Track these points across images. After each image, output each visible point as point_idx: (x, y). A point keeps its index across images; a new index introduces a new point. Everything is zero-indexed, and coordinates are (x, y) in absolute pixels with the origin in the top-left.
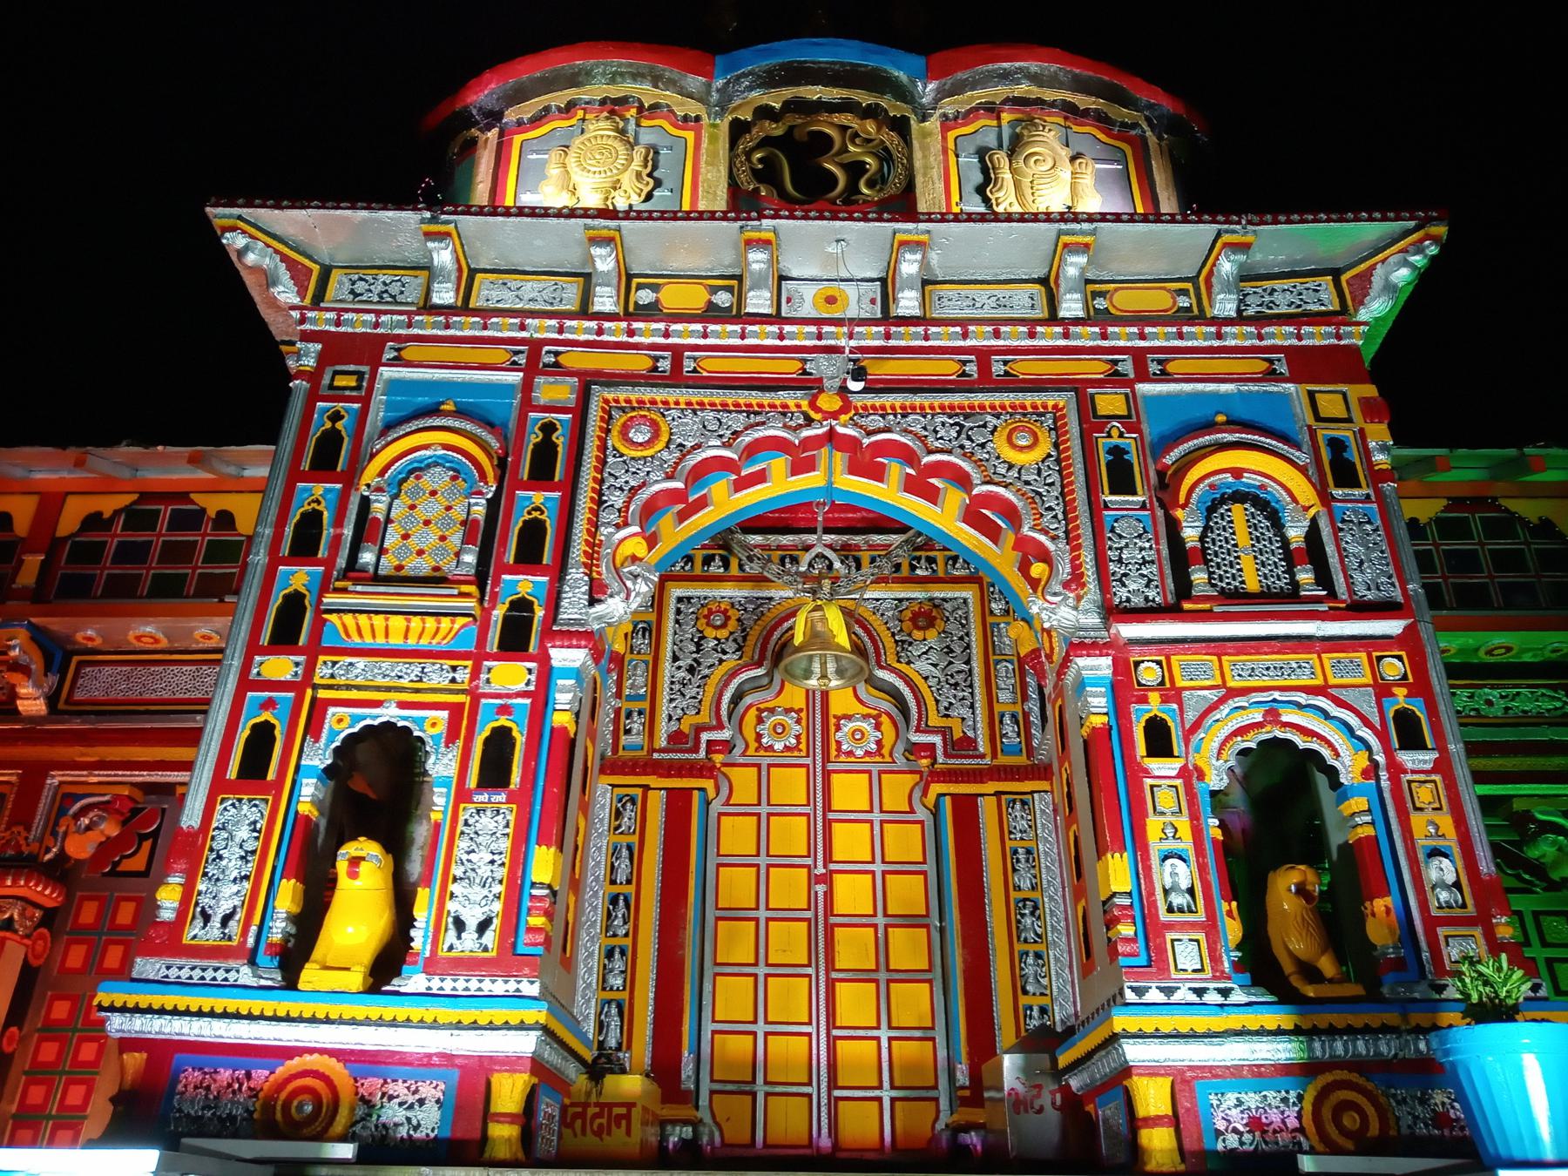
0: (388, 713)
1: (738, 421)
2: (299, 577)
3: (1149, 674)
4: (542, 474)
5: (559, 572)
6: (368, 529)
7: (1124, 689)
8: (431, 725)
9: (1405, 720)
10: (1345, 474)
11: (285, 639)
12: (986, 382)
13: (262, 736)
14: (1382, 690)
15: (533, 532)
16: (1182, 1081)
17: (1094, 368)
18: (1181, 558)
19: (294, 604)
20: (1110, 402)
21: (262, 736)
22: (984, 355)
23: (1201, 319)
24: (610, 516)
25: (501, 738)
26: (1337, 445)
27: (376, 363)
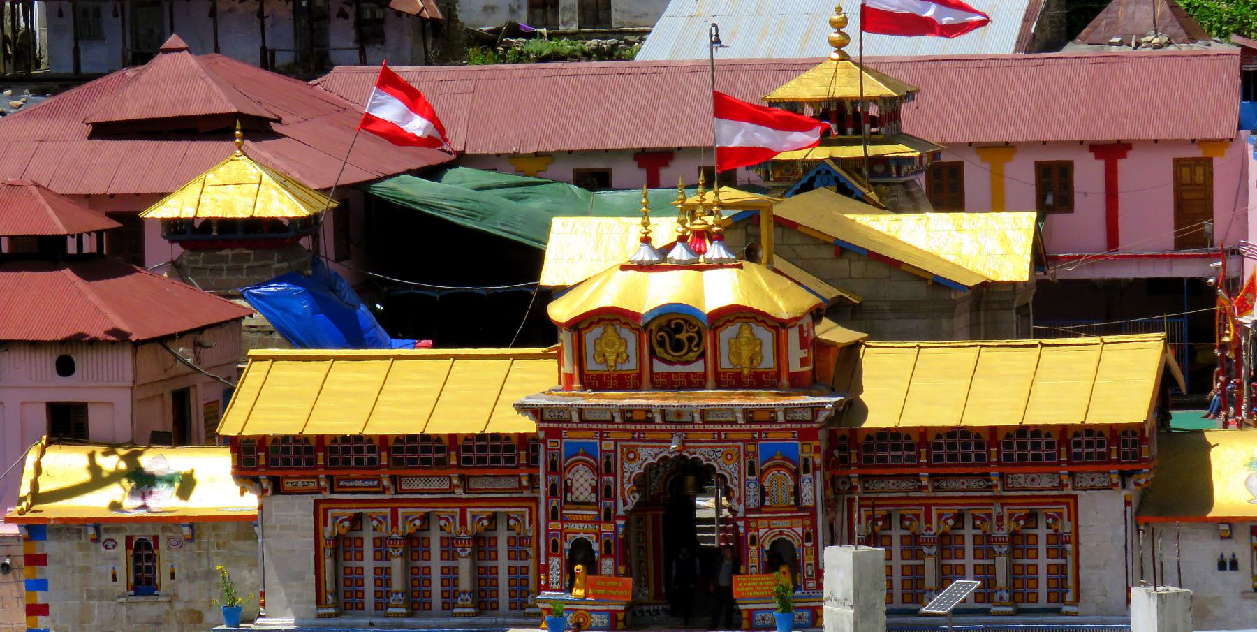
0: (582, 535)
1: (656, 450)
2: (555, 502)
3: (753, 524)
4: (608, 472)
5: (615, 499)
6: (568, 489)
7: (747, 529)
8: (592, 538)
9: (808, 534)
10: (807, 470)
11: (555, 518)
12: (720, 440)
13: (555, 542)
14: (804, 528)
15: (608, 488)
16: (751, 612)
17: (747, 436)
18: (763, 493)
19: (554, 508)
20: (751, 448)
21: (555, 542)
22: (719, 432)
23: (775, 422)
24: (625, 480)
25: (608, 544)
26: (806, 460)
27: (561, 438)
